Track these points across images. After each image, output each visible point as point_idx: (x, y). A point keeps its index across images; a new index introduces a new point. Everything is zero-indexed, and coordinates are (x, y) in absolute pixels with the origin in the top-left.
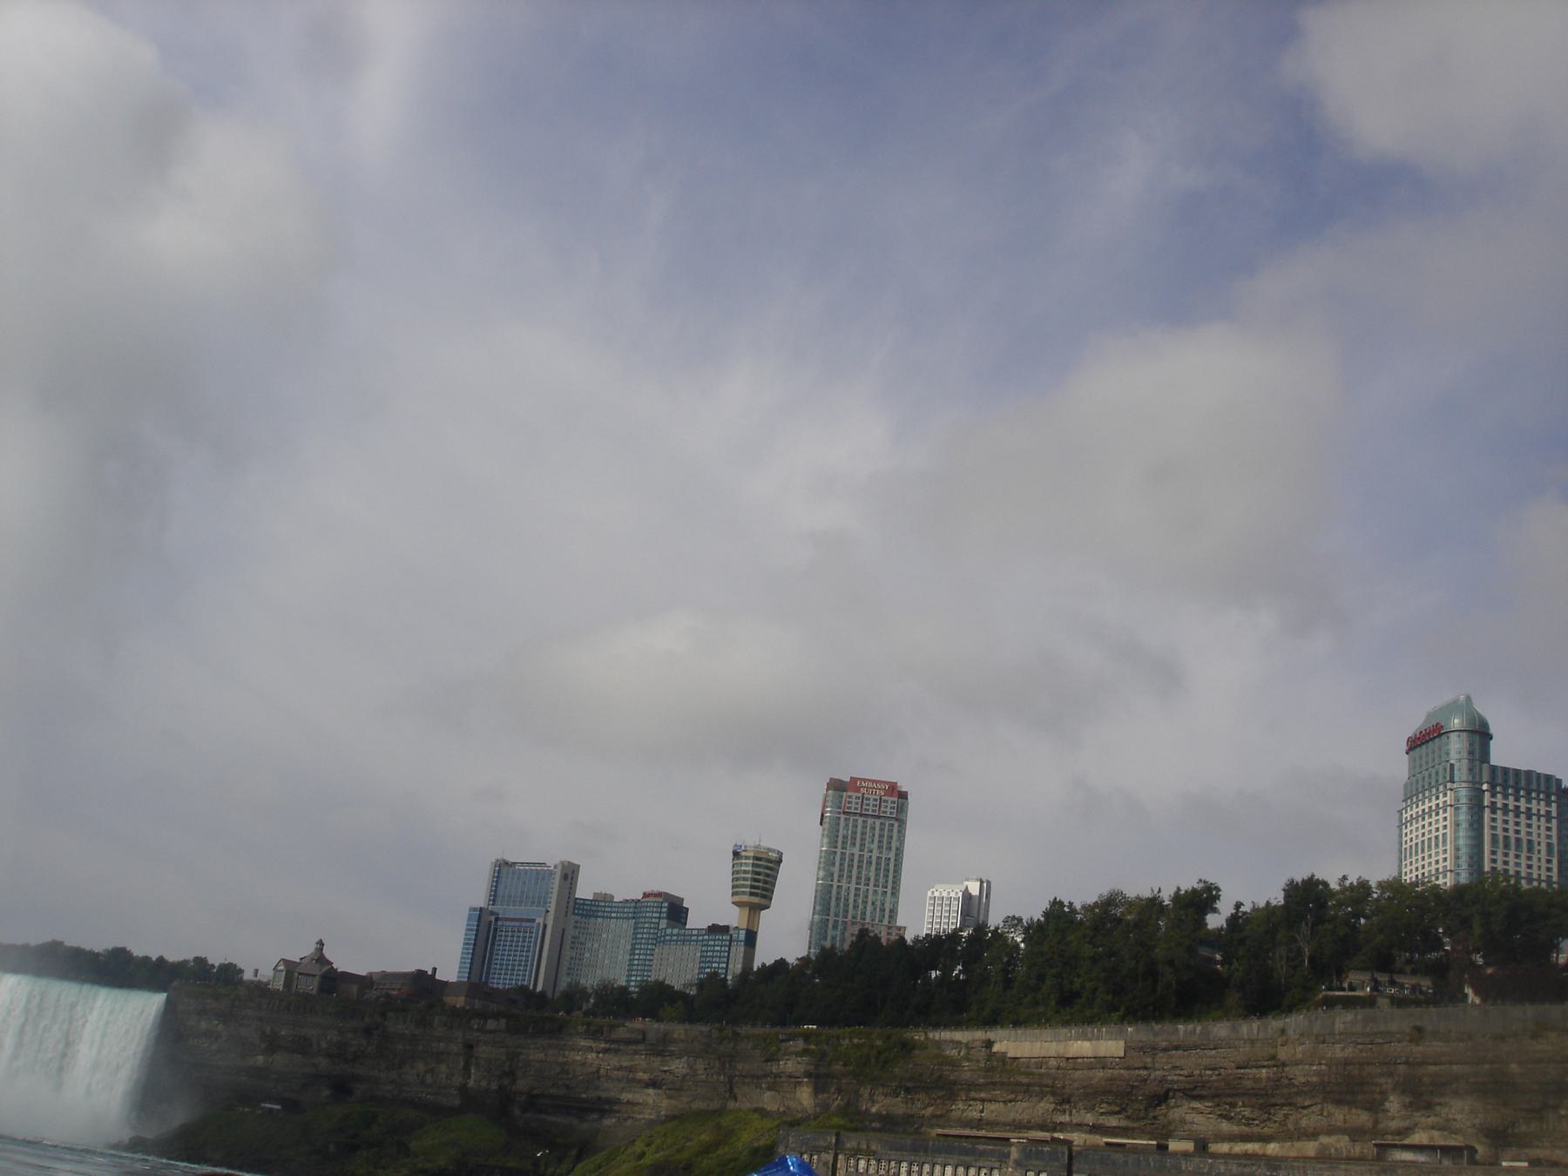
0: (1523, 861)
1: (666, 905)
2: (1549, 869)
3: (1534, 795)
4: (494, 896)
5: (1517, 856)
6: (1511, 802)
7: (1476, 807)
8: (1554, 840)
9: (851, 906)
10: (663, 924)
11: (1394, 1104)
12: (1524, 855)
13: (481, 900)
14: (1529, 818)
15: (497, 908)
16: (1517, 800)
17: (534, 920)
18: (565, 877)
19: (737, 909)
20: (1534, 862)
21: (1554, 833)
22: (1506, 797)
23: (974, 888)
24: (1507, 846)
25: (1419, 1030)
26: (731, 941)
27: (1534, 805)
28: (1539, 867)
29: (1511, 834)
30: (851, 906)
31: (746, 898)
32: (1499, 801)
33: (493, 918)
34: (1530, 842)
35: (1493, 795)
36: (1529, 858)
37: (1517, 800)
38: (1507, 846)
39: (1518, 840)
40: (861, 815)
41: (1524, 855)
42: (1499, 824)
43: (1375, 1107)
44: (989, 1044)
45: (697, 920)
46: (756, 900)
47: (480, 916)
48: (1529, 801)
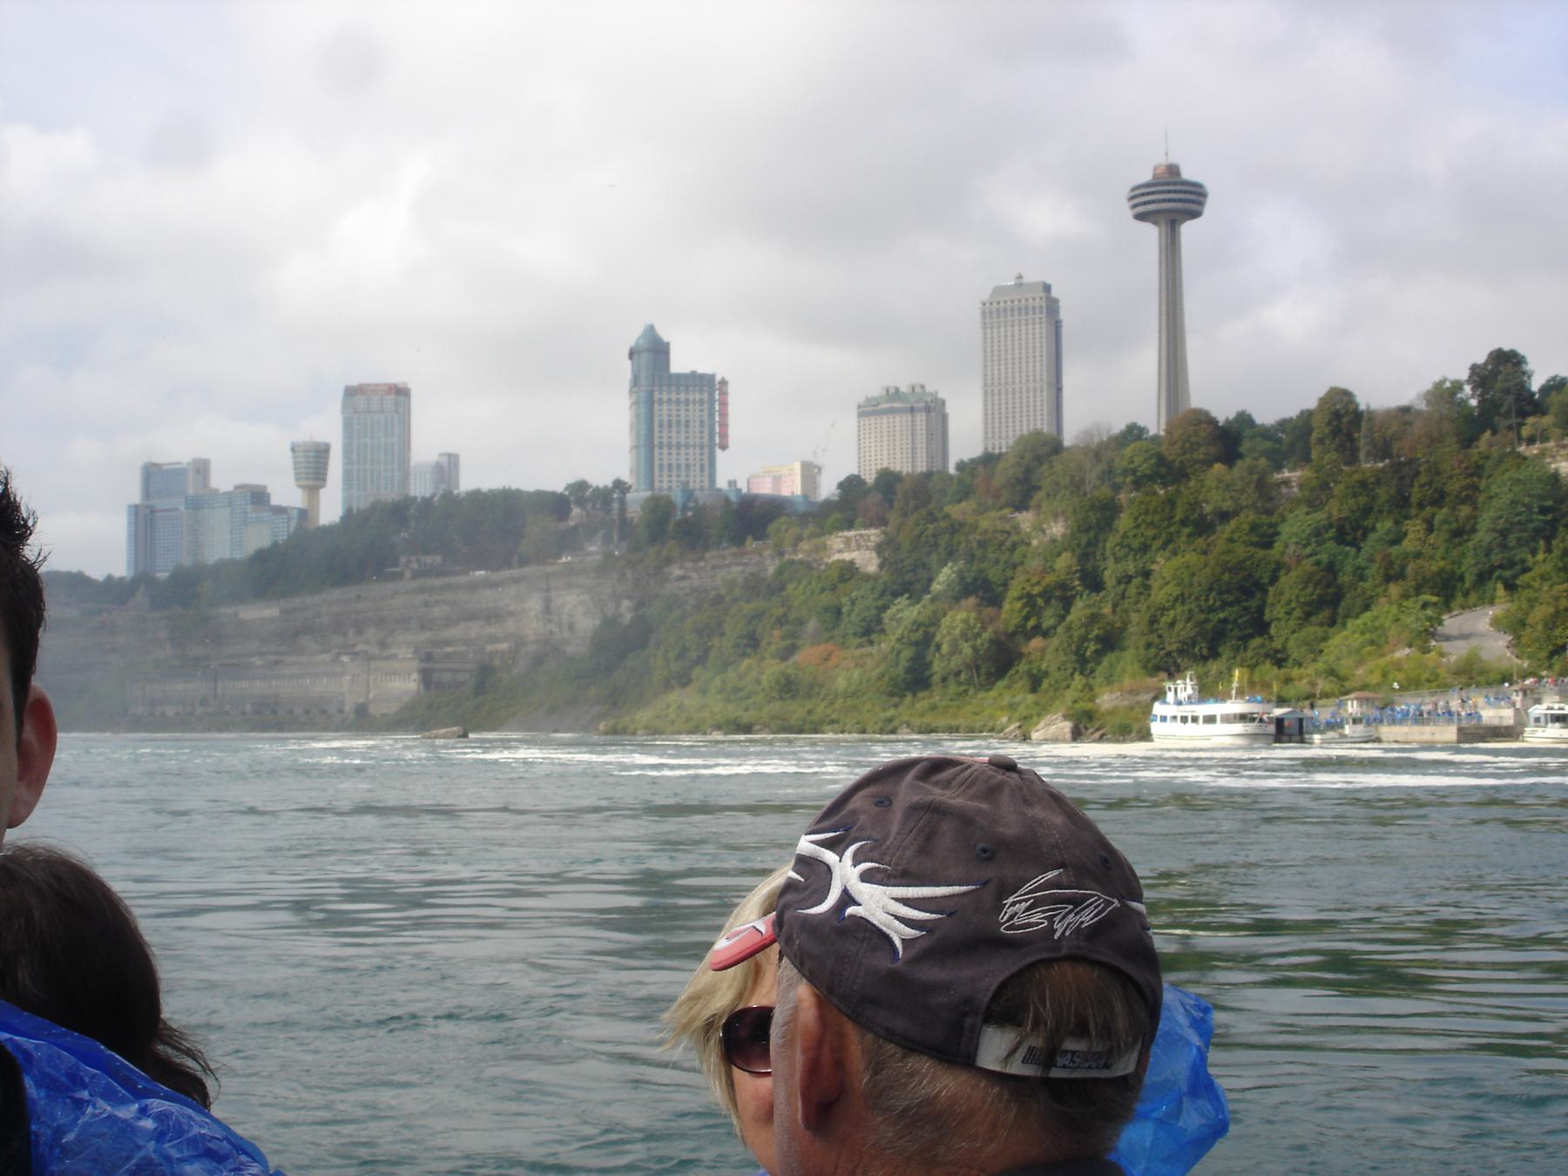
0: (683, 434)
1: (249, 494)
2: (701, 438)
3: (691, 388)
4: (147, 492)
5: (678, 432)
6: (674, 396)
7: (650, 402)
8: (706, 418)
9: (369, 482)
10: (249, 508)
11: (351, 632)
12: (683, 429)
13: (136, 497)
14: (687, 405)
15: (151, 503)
16: (678, 393)
17: (177, 510)
18: (198, 471)
19: (300, 490)
20: (691, 435)
21: (706, 413)
22: (669, 392)
23: (444, 460)
24: (670, 426)
25: (359, 596)
26: (288, 518)
27: (691, 397)
28: (694, 437)
29: (674, 418)
30: (369, 482)
31: (304, 483)
32: (665, 397)
33: (148, 511)
34: (687, 421)
35: (661, 393)
36: (687, 432)
37: (678, 393)
38: (670, 426)
39: (678, 422)
40: (369, 412)
41: (683, 429)
42: (665, 413)
43: (345, 634)
44: (236, 614)
45: (276, 500)
46: (311, 483)
47: (136, 514)
48: (687, 391)
